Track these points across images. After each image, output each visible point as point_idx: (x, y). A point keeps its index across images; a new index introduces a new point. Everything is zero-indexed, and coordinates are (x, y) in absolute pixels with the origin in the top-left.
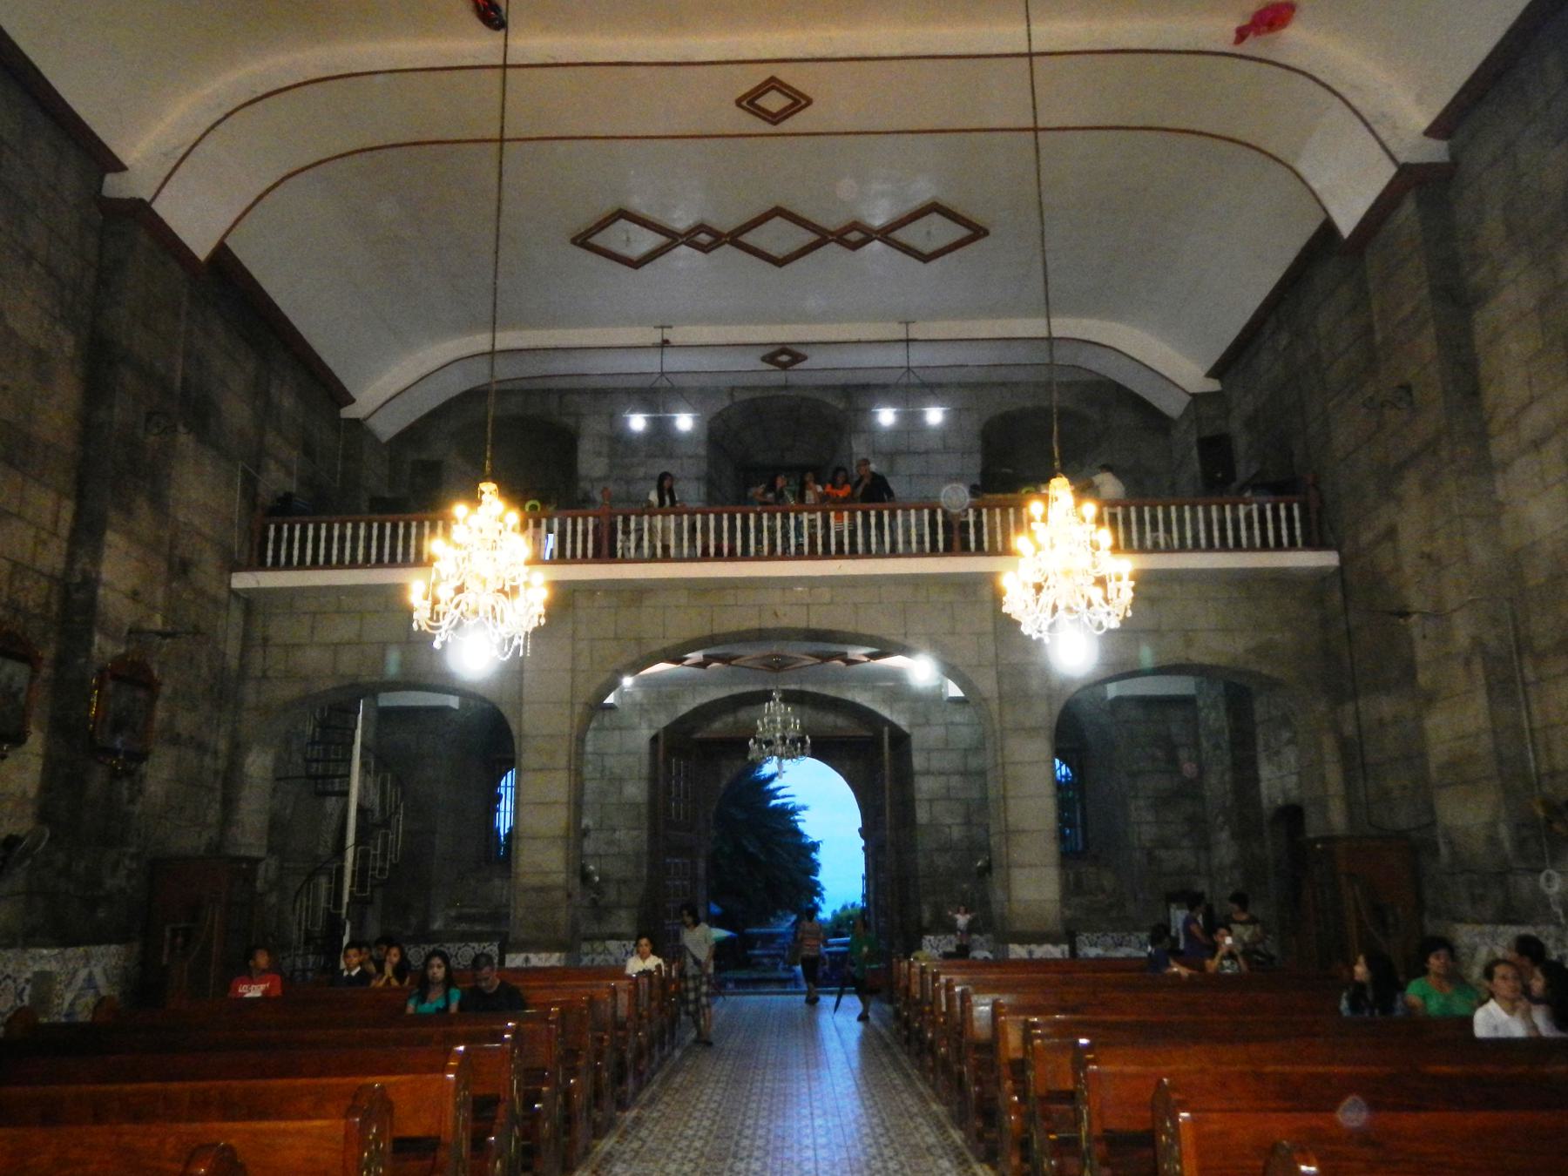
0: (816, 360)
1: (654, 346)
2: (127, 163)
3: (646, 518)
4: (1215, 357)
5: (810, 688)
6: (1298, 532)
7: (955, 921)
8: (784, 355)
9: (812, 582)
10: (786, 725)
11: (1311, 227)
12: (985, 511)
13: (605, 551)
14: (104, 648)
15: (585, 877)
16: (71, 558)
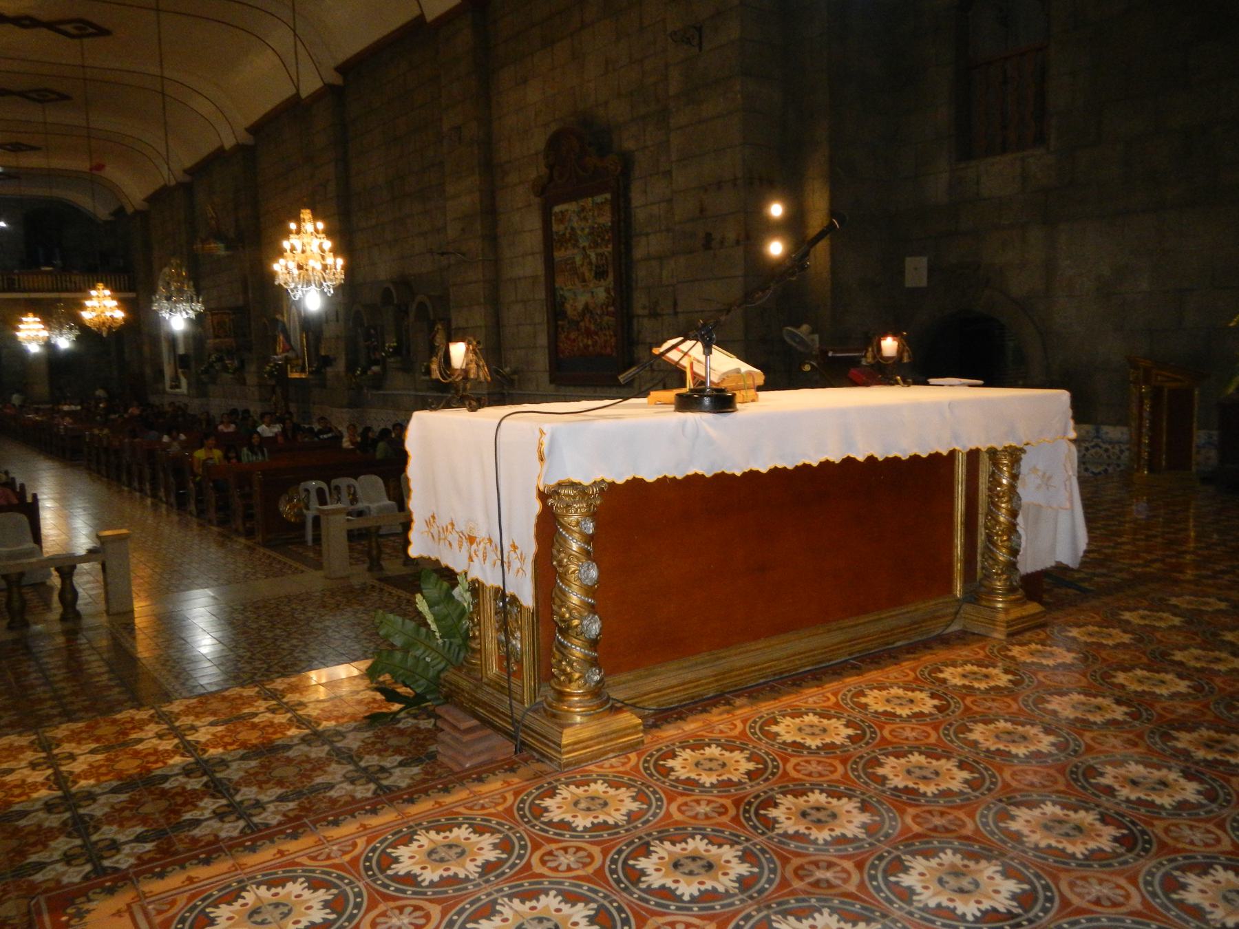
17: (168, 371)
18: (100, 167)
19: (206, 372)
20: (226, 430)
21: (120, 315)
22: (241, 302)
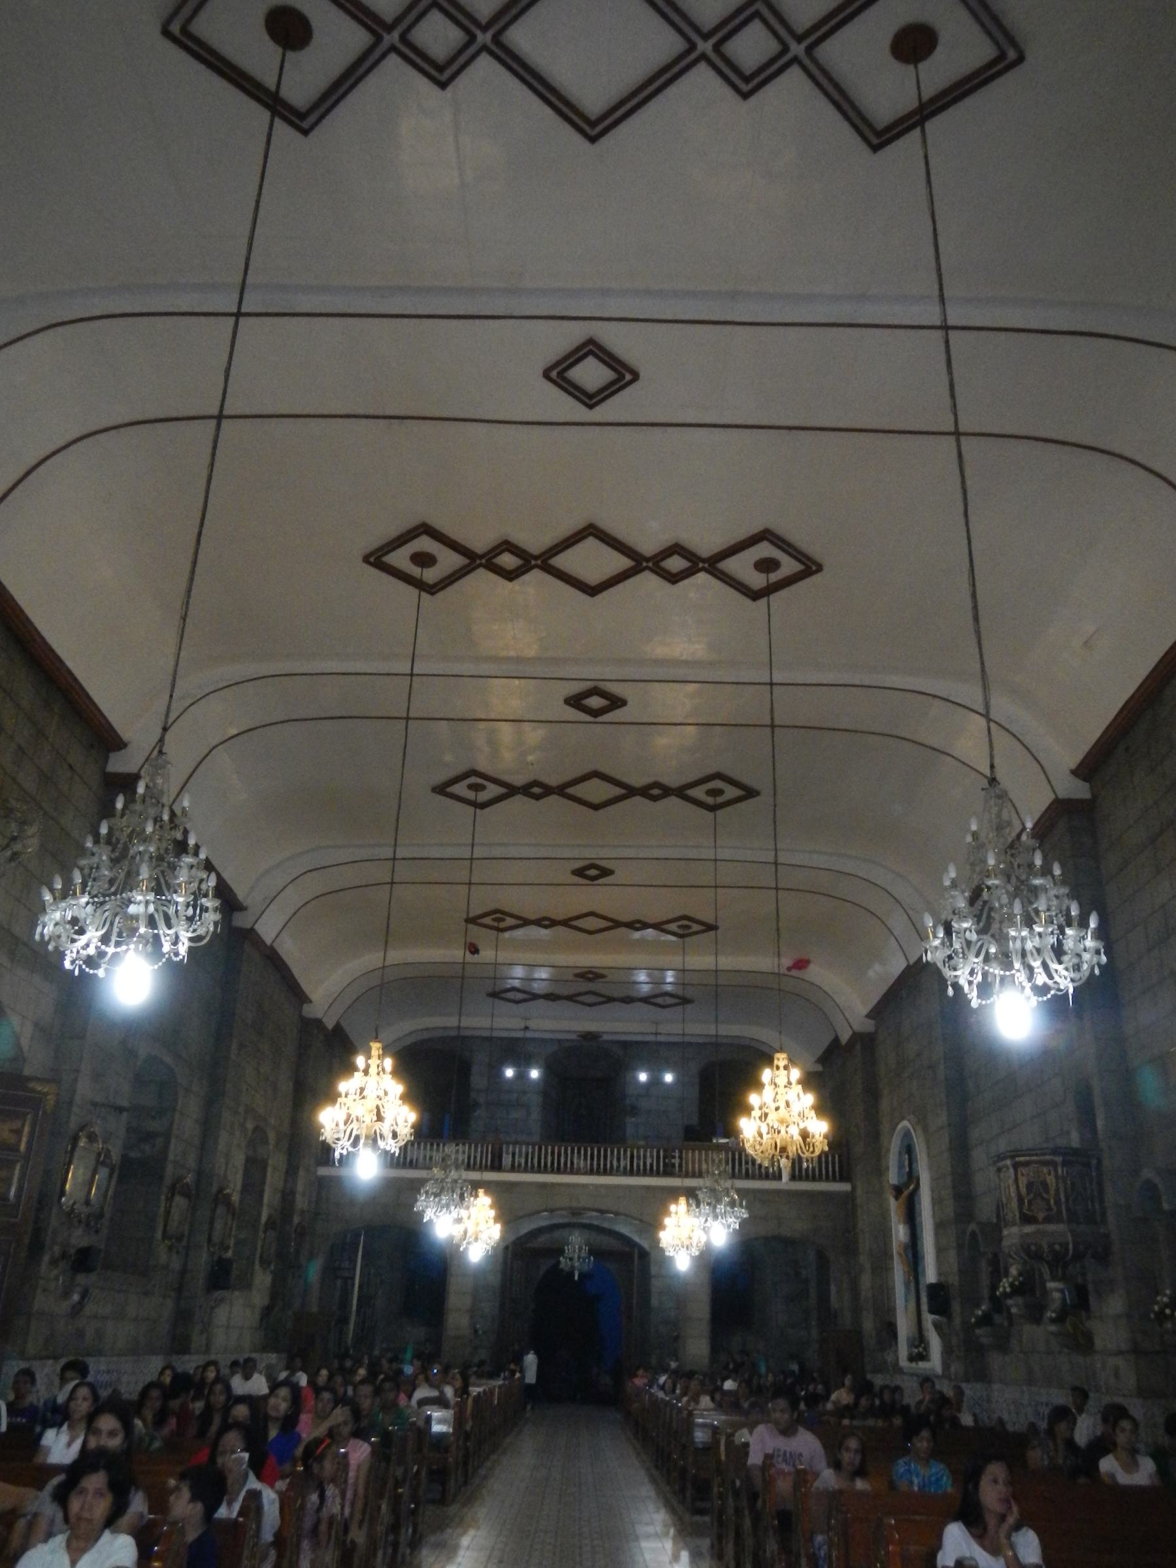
0: (606, 1037)
1: (521, 1030)
2: (313, 1000)
3: (518, 1146)
4: (820, 1052)
5: (596, 1223)
6: (837, 1169)
7: (669, 1365)
8: (590, 1037)
9: (597, 1187)
10: (580, 1249)
11: (833, 1037)
12: (684, 1152)
13: (496, 1164)
14: (296, 1220)
15: (476, 1331)
16: (286, 1181)
17: (904, 1327)
18: (801, 964)
19: (986, 1320)
20: (1123, 1479)
21: (820, 1128)
22: (1075, 1140)
